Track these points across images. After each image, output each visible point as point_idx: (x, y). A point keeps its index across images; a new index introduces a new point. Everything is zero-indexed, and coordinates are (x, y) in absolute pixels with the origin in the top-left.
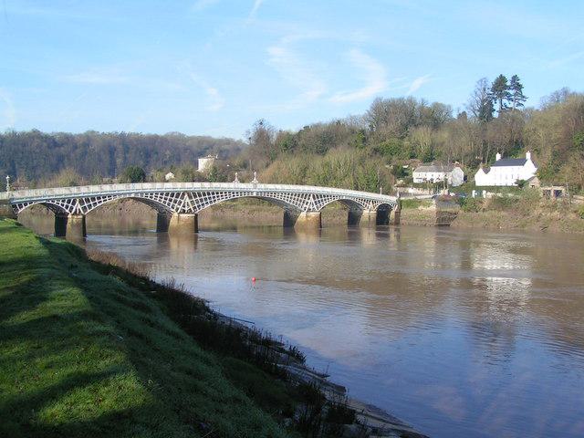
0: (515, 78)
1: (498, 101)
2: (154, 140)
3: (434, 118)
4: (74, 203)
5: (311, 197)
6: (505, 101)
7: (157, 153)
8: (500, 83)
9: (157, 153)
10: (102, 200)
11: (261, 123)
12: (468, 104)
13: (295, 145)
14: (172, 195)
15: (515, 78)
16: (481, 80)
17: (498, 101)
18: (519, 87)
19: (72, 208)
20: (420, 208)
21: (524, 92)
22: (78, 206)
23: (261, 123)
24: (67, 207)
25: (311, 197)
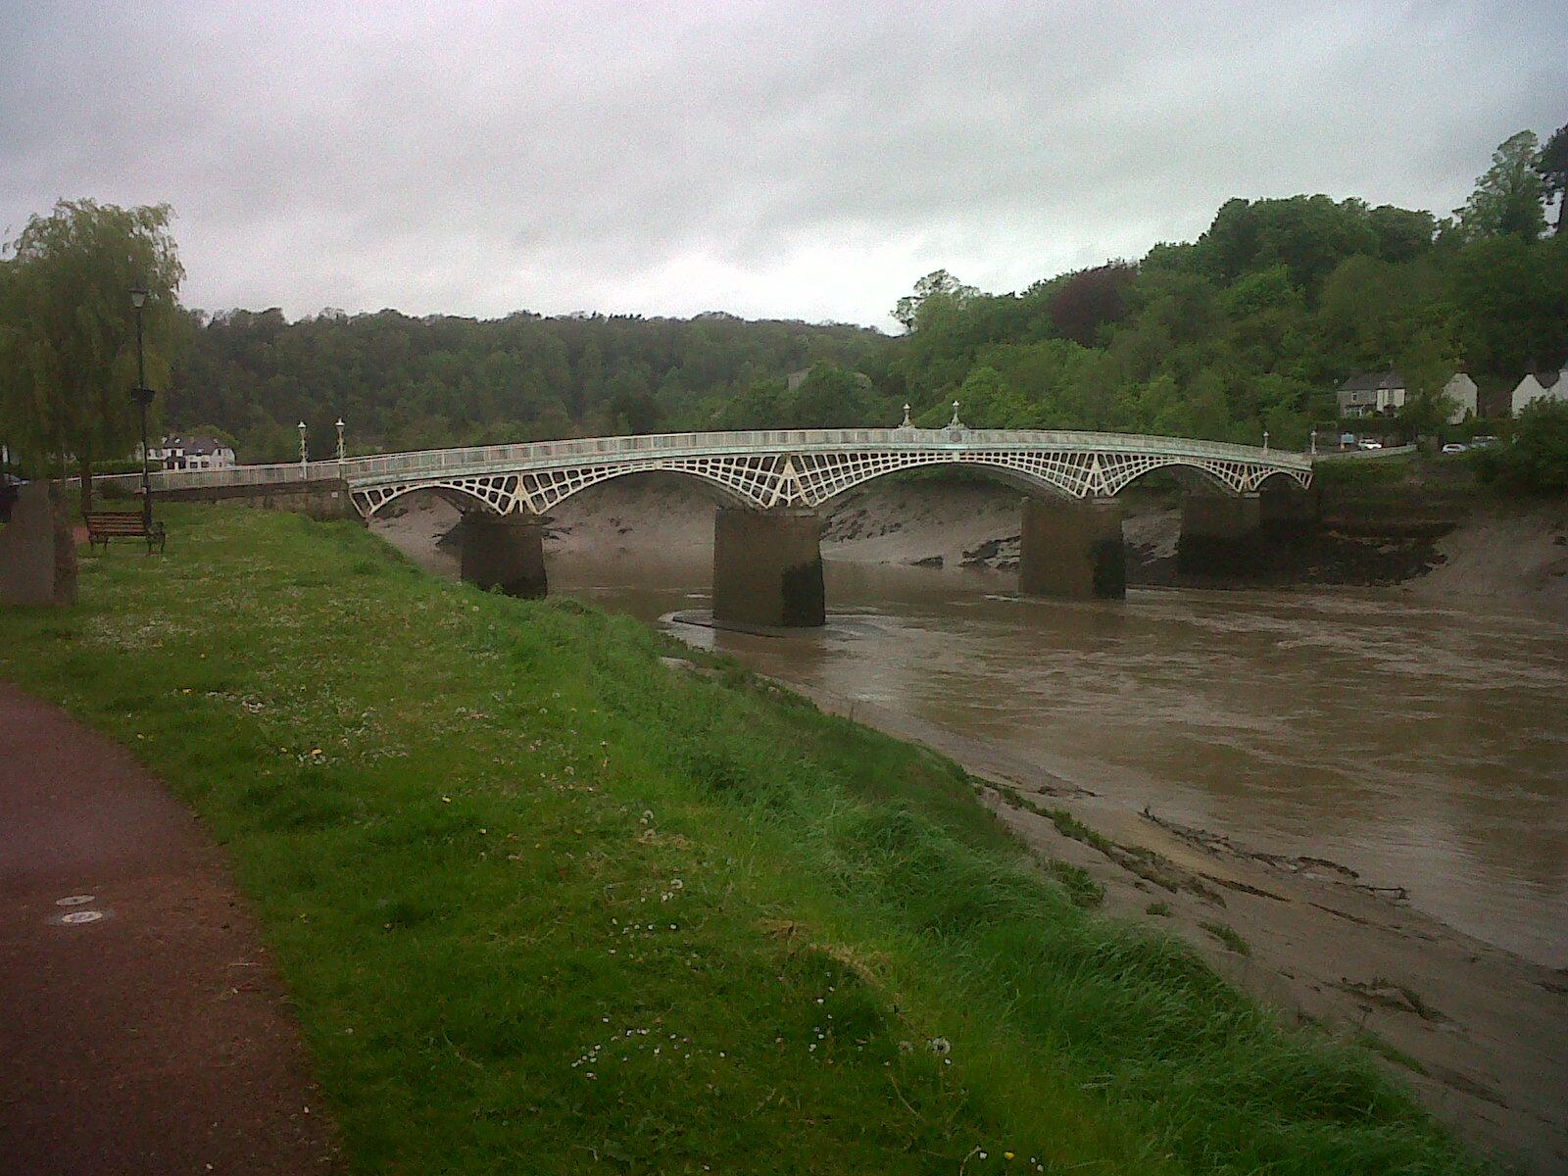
4: (510, 488)
5: (1096, 464)
10: (581, 478)
11: (937, 284)
22: (521, 494)
24: (493, 497)
25: (1096, 464)
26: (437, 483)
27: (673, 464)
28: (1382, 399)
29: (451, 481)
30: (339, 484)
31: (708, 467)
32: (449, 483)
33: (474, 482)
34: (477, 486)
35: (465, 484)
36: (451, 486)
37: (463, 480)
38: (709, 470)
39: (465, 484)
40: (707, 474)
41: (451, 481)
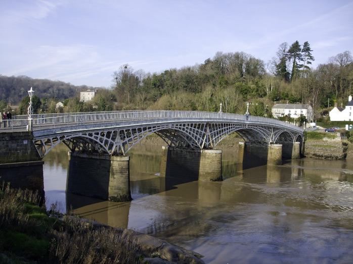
0: (306, 44)
1: (292, 60)
2: (12, 79)
3: (252, 69)
6: (297, 60)
7: (14, 89)
8: (296, 47)
9: (14, 89)
11: (126, 67)
12: (272, 60)
13: (162, 85)
14: (192, 125)
15: (306, 44)
16: (283, 44)
17: (292, 60)
18: (307, 49)
19: (111, 145)
20: (325, 139)
21: (313, 54)
22: (118, 142)
23: (126, 67)
26: (80, 135)
27: (175, 126)
28: (286, 112)
29: (87, 133)
30: (28, 135)
31: (185, 128)
32: (86, 134)
33: (98, 134)
34: (99, 136)
35: (94, 135)
36: (87, 136)
37: (93, 133)
38: (186, 129)
39: (94, 135)
40: (185, 132)
41: (87, 133)
